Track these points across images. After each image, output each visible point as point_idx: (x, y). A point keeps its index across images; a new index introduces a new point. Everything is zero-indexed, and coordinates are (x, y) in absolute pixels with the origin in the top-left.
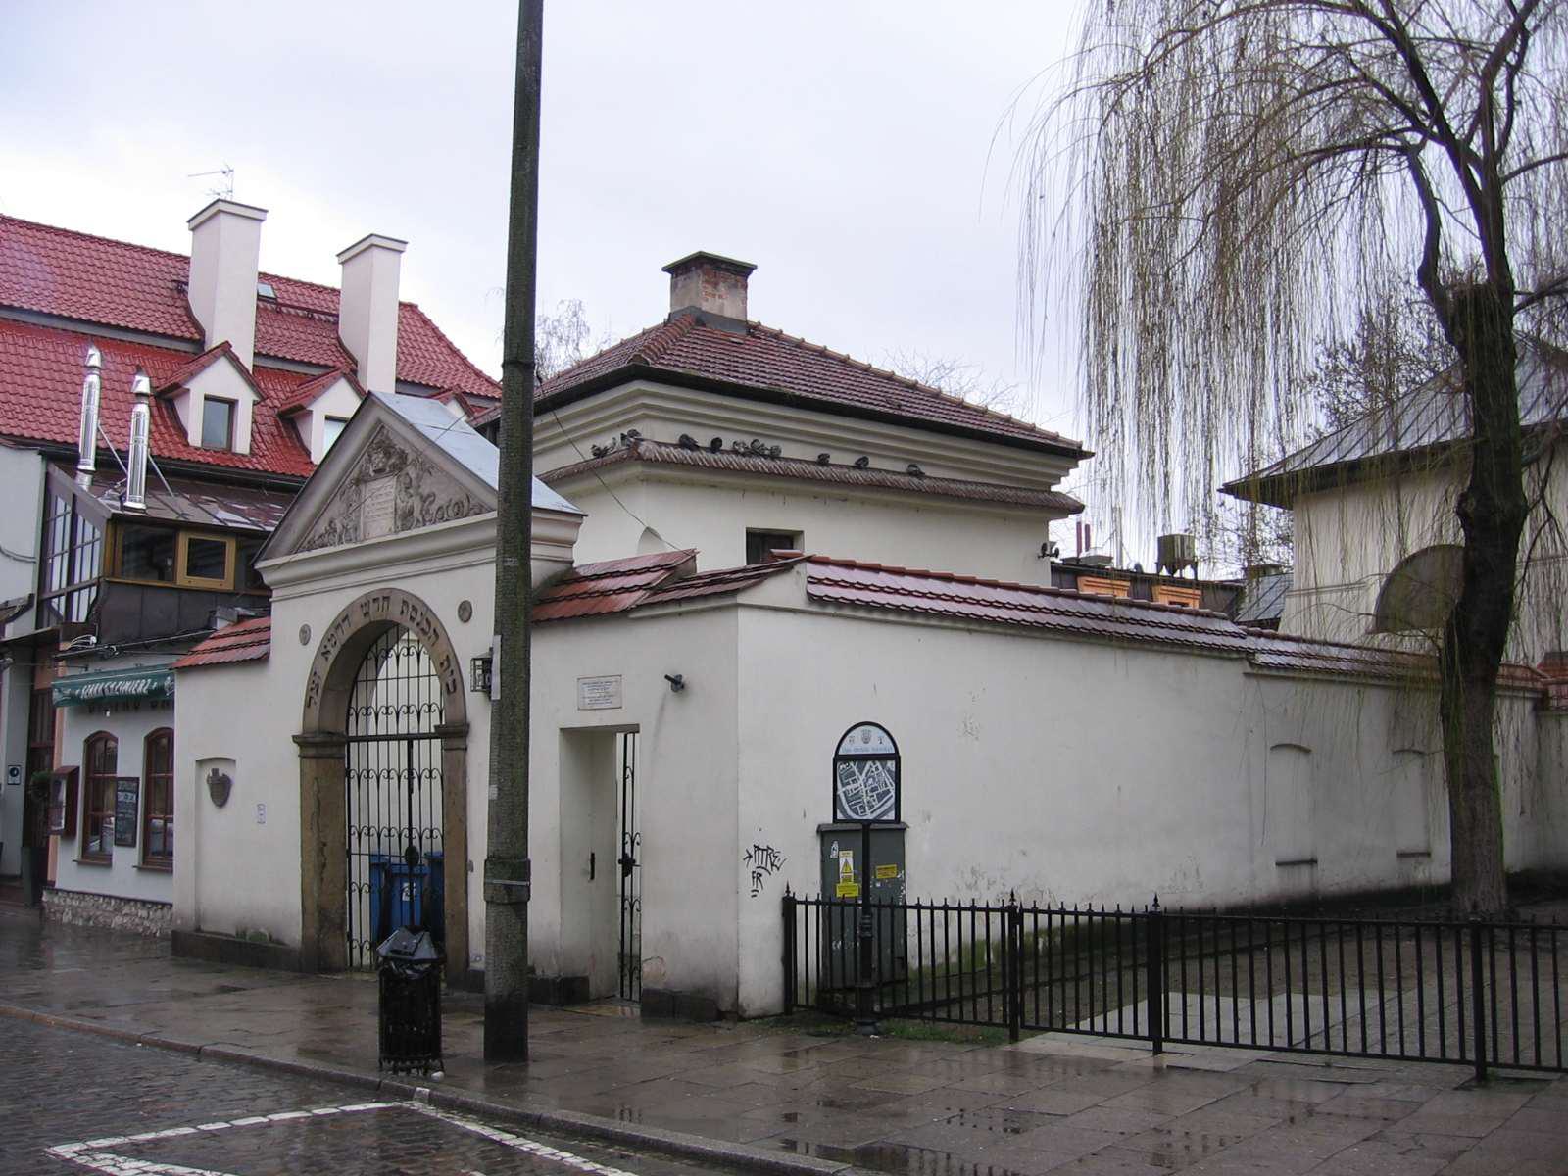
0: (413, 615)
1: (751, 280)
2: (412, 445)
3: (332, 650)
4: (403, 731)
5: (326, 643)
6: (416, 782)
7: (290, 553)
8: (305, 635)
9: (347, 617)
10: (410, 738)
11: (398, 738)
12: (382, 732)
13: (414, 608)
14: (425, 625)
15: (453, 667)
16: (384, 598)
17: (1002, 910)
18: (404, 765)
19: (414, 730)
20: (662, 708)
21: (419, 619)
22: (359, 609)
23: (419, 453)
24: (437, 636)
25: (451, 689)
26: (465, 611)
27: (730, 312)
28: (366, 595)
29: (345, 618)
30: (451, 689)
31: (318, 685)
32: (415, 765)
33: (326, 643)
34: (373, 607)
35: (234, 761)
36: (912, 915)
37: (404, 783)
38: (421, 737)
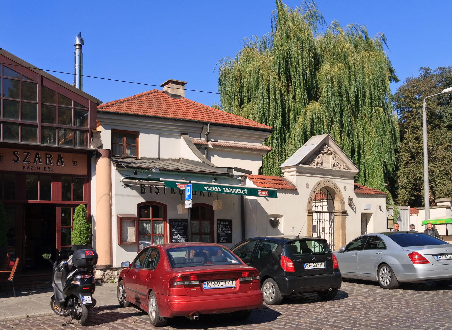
3: (316, 191)
4: (319, 211)
6: (321, 222)
8: (308, 186)
10: (320, 212)
12: (324, 211)
13: (335, 185)
16: (329, 182)
18: (319, 218)
19: (321, 211)
21: (336, 188)
32: (321, 218)
34: (326, 183)
37: (319, 222)
38: (323, 212)
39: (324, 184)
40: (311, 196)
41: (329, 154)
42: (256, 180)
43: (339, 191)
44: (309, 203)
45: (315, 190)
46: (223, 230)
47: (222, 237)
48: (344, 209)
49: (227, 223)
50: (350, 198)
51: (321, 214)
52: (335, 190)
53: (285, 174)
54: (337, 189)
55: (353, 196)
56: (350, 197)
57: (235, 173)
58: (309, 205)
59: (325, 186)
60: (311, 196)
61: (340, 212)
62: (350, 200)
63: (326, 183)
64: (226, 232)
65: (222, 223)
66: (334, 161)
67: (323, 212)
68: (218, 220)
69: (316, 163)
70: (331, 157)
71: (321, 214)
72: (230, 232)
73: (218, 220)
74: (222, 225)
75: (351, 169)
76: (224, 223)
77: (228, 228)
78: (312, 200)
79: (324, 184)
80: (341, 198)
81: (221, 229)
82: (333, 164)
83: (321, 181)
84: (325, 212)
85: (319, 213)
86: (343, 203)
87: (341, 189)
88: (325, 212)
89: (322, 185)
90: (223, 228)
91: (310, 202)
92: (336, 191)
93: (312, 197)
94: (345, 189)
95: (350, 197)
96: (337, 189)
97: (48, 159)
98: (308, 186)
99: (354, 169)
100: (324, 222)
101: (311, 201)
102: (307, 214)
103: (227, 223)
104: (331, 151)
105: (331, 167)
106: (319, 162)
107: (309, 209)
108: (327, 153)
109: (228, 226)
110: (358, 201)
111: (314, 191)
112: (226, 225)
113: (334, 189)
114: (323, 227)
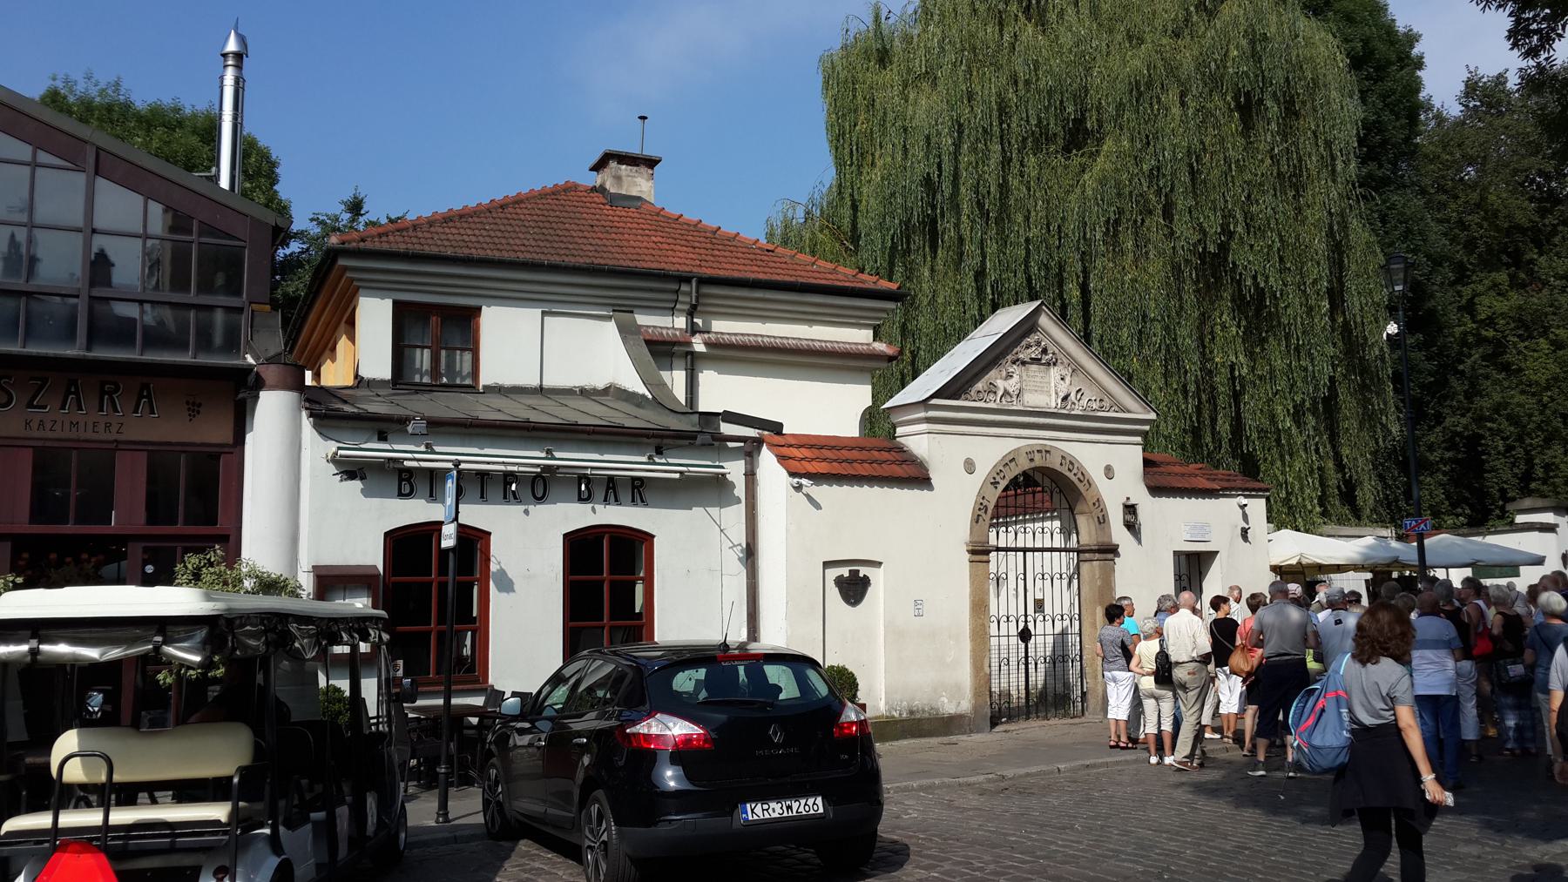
0: (1071, 467)
4: (1020, 544)
5: (995, 475)
8: (970, 466)
10: (1025, 550)
11: (1016, 550)
12: (1039, 545)
13: (1071, 463)
16: (1047, 452)
19: (1030, 545)
21: (1075, 471)
24: (1090, 484)
29: (1010, 460)
33: (995, 475)
34: (1037, 457)
37: (1021, 583)
38: (1034, 550)
39: (1032, 460)
40: (983, 498)
41: (1048, 364)
42: (898, 456)
43: (1086, 481)
44: (977, 522)
45: (998, 479)
48: (1106, 540)
50: (1132, 502)
51: (1028, 553)
52: (1074, 479)
53: (900, 431)
54: (1080, 475)
55: (1141, 496)
56: (1128, 499)
57: (727, 429)
58: (977, 527)
59: (1033, 465)
60: (983, 498)
61: (1093, 548)
62: (1130, 509)
63: (1037, 457)
66: (1063, 388)
67: (1034, 550)
69: (1000, 393)
70: (1055, 372)
71: (1029, 554)
75: (1129, 412)
78: (986, 512)
80: (1098, 502)
82: (1062, 395)
83: (1019, 448)
84: (1052, 550)
85: (1020, 554)
86: (1103, 521)
87: (1097, 475)
88: (1052, 550)
89: (1025, 464)
91: (981, 519)
92: (1076, 482)
93: (985, 503)
94: (1109, 472)
95: (1128, 499)
96: (1080, 475)
97: (106, 397)
98: (970, 466)
99: (1140, 410)
100: (1039, 583)
101: (984, 515)
102: (968, 556)
104: (1054, 354)
105: (1054, 405)
106: (1011, 391)
107: (975, 539)
108: (1040, 359)
110: (1152, 509)
111: (995, 484)
113: (1070, 475)
114: (1039, 596)
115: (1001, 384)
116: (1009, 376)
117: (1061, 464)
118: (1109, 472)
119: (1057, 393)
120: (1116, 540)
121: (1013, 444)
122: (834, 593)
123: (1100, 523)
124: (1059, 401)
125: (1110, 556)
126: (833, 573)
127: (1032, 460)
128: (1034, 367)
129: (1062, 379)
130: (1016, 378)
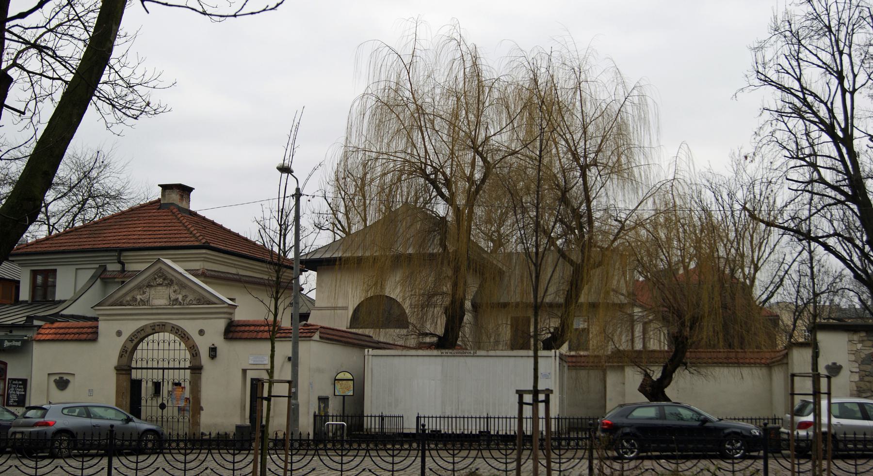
0: (177, 331)
1: (192, 194)
2: (175, 278)
7: (109, 306)
8: (119, 333)
9: (143, 330)
10: (163, 369)
13: (177, 329)
14: (183, 336)
15: (195, 348)
16: (163, 325)
17: (379, 416)
20: (283, 366)
21: (180, 333)
22: (150, 328)
23: (179, 280)
24: (188, 339)
25: (195, 355)
26: (201, 332)
27: (186, 207)
28: (154, 323)
30: (195, 355)
31: (126, 351)
35: (74, 374)
36: (365, 418)
44: (121, 357)
45: (133, 338)
46: (15, 391)
47: (12, 399)
48: (197, 364)
49: (20, 382)
54: (183, 335)
64: (18, 393)
65: (14, 382)
68: (9, 379)
72: (23, 393)
73: (9, 379)
74: (14, 384)
76: (16, 382)
77: (21, 388)
79: (153, 329)
81: (12, 389)
83: (146, 325)
90: (15, 388)
93: (126, 349)
95: (213, 345)
98: (119, 333)
103: (20, 382)
109: (22, 386)
112: (20, 384)
115: (139, 297)
116: (144, 293)
117: (171, 330)
118: (201, 332)
119: (170, 298)
120: (203, 363)
121: (143, 323)
122: (53, 386)
123: (194, 356)
124: (171, 303)
125: (197, 372)
126: (53, 378)
127: (153, 329)
128: (160, 288)
129: (174, 292)
130: (147, 294)
